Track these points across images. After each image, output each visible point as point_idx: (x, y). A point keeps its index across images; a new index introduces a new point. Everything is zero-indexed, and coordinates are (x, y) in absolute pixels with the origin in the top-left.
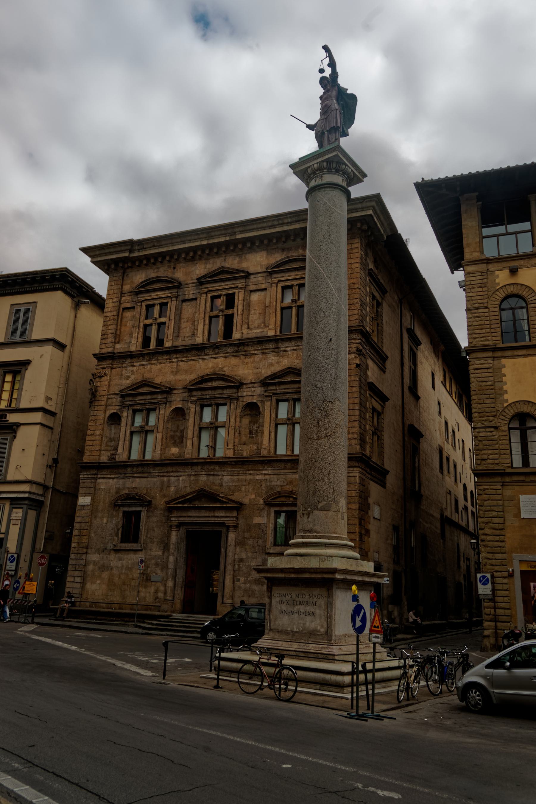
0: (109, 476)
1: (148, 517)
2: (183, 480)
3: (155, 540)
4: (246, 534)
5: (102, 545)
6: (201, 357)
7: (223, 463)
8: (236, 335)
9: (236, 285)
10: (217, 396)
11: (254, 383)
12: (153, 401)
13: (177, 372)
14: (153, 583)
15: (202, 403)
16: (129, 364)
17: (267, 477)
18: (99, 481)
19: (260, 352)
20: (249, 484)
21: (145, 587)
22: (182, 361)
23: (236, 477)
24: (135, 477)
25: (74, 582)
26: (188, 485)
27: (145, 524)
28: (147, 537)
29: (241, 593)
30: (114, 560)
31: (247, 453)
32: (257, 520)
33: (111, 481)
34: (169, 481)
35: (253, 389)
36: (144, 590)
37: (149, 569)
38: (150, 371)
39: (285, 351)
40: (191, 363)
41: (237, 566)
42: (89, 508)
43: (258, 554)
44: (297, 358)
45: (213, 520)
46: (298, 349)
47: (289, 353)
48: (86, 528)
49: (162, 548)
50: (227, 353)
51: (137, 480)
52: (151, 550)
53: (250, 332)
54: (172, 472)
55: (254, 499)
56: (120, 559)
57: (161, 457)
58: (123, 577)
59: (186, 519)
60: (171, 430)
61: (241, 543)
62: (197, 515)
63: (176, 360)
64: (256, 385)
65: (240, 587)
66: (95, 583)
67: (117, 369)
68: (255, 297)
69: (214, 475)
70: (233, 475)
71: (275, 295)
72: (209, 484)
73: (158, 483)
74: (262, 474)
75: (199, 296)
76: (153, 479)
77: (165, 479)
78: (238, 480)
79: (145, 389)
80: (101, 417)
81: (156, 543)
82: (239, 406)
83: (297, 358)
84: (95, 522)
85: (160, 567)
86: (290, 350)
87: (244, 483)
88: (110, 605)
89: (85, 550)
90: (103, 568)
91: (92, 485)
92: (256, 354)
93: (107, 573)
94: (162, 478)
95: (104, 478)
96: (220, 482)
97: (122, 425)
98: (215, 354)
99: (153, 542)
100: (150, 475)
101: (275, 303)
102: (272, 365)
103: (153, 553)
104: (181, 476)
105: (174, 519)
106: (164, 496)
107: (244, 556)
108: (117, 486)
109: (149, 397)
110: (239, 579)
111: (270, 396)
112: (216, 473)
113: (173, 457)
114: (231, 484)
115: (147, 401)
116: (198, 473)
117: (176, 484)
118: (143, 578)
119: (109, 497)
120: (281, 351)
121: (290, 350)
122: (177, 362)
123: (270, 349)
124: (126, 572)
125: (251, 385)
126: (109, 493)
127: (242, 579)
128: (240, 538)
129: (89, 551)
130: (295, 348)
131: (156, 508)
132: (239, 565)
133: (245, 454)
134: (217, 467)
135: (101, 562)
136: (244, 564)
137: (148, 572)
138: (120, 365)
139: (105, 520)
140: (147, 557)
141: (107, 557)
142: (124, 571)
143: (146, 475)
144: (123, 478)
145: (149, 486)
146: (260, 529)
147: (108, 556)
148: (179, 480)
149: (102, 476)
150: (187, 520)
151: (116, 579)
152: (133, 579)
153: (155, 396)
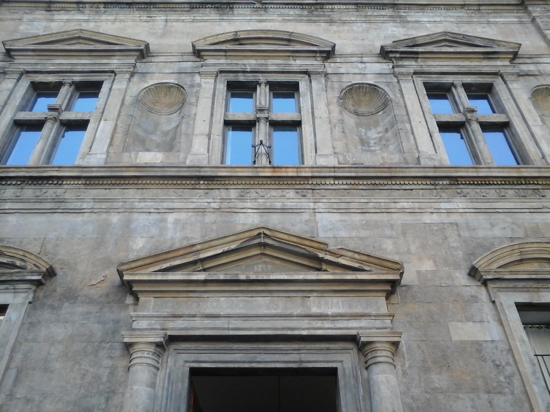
2: (177, 222)
11: (362, 56)
12: (96, 68)
13: (163, 35)
20: (404, 234)
23: (357, 218)
27: (13, 350)
32: (463, 332)
34: (127, 224)
40: (201, 24)
45: (304, 328)
55: (433, 272)
57: (106, 162)
60: (139, 126)
69: (284, 210)
70: (347, 211)
73: (90, 228)
74: (438, 211)
77: (115, 218)
78: (367, 225)
82: (333, 88)
86: (429, 22)
87: (388, 232)
92: (353, 22)
94: (104, 216)
100: (60, 207)
104: (171, 210)
114: (343, 234)
115: (79, 68)
120: (408, 22)
121: (429, 22)
122: (166, 21)
128: (416, 391)
131: (71, 296)
143: (48, 206)
145: (52, 235)
146: (484, 360)
148: (164, 220)
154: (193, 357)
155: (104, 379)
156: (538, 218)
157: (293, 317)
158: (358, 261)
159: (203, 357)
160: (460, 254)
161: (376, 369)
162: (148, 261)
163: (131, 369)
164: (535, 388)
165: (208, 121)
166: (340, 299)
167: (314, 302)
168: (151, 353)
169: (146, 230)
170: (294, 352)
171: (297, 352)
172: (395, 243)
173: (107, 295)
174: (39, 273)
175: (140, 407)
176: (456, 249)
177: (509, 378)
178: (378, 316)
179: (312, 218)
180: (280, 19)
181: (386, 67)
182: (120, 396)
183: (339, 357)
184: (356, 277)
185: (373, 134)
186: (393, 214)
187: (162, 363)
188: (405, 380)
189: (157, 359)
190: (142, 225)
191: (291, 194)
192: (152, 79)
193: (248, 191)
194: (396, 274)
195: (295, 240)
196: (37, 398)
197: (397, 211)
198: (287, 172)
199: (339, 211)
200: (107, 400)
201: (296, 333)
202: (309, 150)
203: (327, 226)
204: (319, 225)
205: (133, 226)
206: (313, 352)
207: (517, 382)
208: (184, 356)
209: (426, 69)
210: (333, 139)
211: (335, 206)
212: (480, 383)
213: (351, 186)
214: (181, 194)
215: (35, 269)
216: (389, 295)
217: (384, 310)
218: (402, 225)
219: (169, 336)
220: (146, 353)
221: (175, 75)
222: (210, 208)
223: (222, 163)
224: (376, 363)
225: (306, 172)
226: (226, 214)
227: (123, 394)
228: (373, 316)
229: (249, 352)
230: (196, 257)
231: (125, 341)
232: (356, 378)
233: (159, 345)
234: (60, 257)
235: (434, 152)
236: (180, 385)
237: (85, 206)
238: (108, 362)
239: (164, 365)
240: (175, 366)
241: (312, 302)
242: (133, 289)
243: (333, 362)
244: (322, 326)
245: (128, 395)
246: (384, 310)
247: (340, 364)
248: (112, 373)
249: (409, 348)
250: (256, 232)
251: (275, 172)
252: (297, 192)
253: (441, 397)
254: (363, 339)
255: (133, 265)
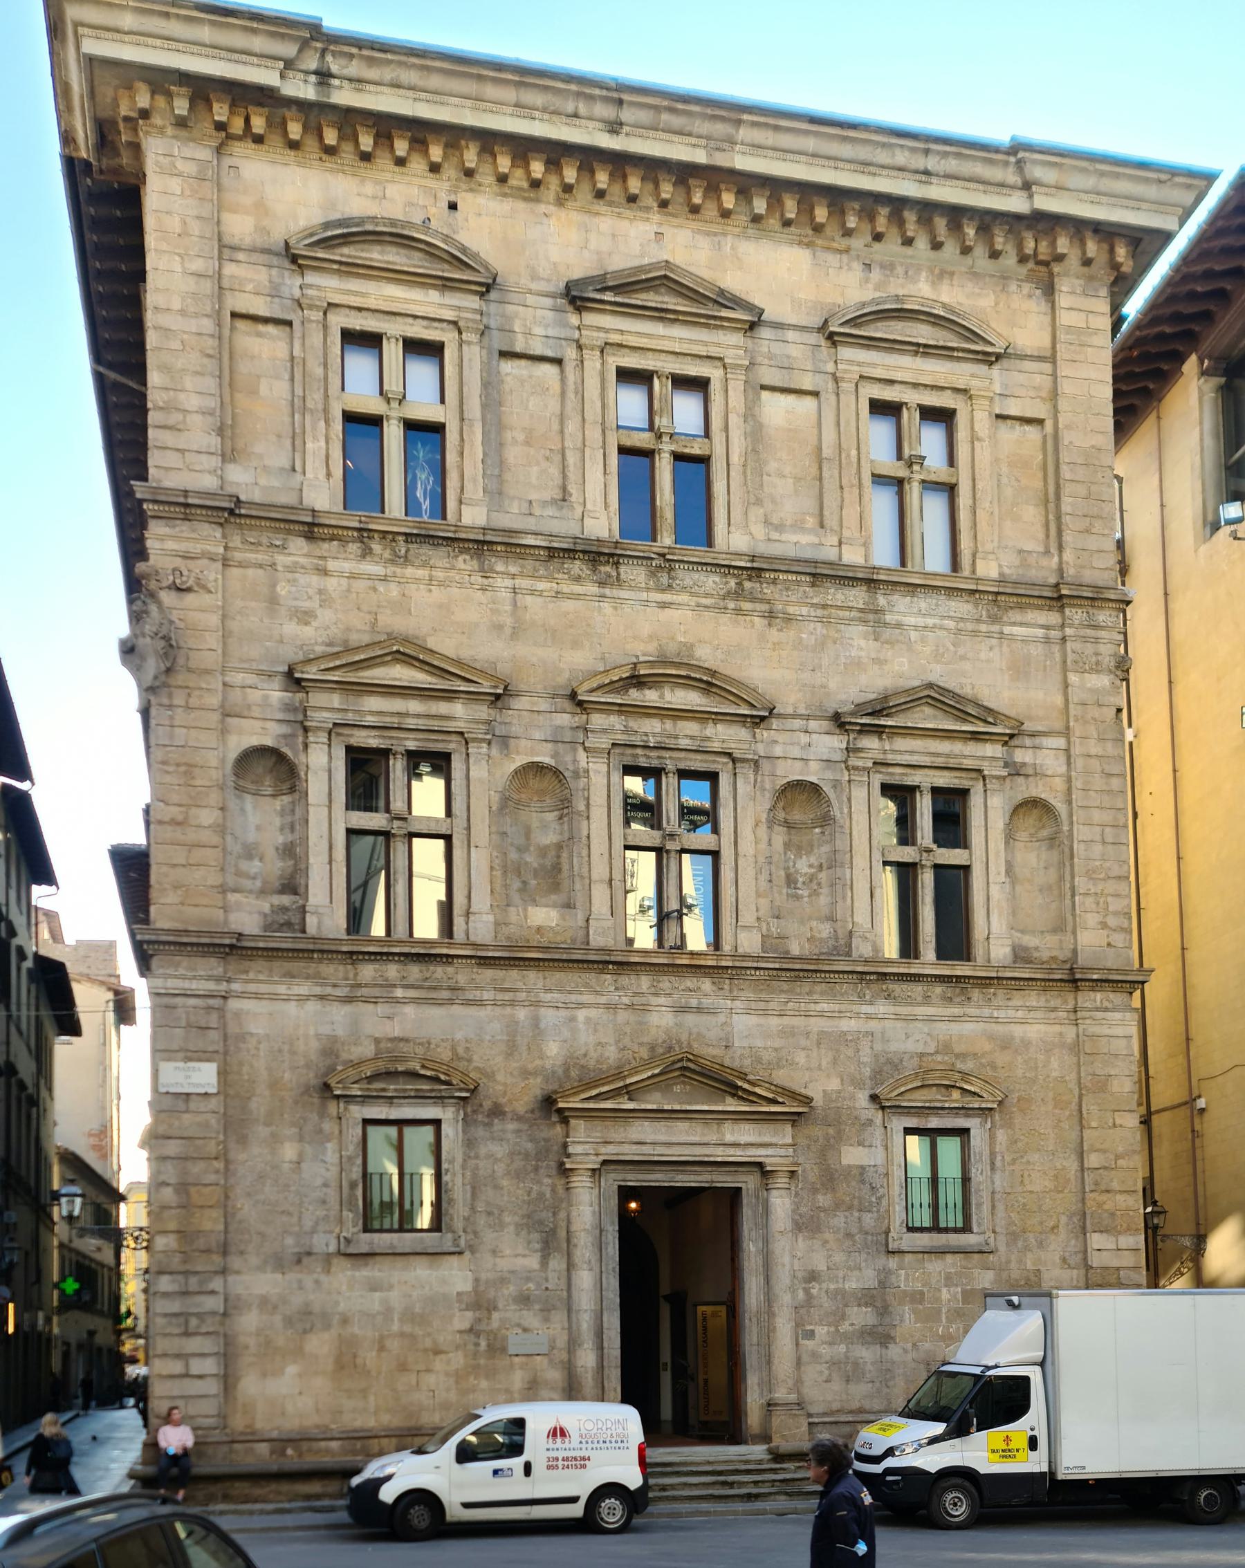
0: (282, 989)
1: (470, 1143)
2: (588, 1020)
3: (507, 1219)
4: (820, 1197)
5: (289, 1241)
6: (607, 591)
7: (717, 968)
8: (735, 536)
9: (714, 351)
10: (684, 743)
13: (516, 633)
14: (516, 1359)
15: (629, 761)
16: (302, 560)
17: (873, 1025)
18: (233, 1004)
19: (819, 612)
20: (819, 1044)
21: (491, 1374)
22: (533, 592)
23: (774, 1021)
24: (397, 1001)
25: (187, 1375)
26: (612, 1041)
27: (464, 1167)
28: (473, 1208)
29: (821, 1372)
30: (347, 1289)
31: (802, 948)
32: (852, 1156)
33: (292, 1008)
34: (536, 1022)
35: (805, 739)
36: (484, 1384)
37: (496, 1316)
38: (402, 606)
39: (899, 625)
40: (569, 605)
41: (801, 1295)
42: (213, 1104)
43: (864, 1256)
44: (937, 656)
45: (720, 1154)
46: (942, 628)
47: (914, 635)
48: (212, 1178)
49: (538, 1246)
50: (707, 595)
51: (409, 1010)
52: (494, 1252)
53: (775, 535)
54: (550, 991)
55: (839, 1092)
56: (374, 1287)
58: (394, 1345)
60: (512, 844)
61: (806, 1225)
62: (662, 1138)
63: (509, 582)
64: (813, 725)
65: (815, 1355)
66: (279, 1372)
67: (250, 572)
68: (776, 408)
69: (699, 1010)
70: (765, 1013)
71: (853, 424)
72: (684, 1038)
73: (496, 1026)
75: (570, 353)
76: (472, 1011)
77: (522, 1014)
79: (400, 674)
80: (212, 759)
81: (512, 1228)
82: (763, 789)
83: (937, 656)
84: (242, 1157)
85: (537, 1307)
88: (359, 1444)
89: (217, 1259)
90: (306, 1320)
91: (213, 1020)
93: (326, 1336)
94: (508, 1010)
95: (257, 996)
96: (722, 1035)
97: (312, 799)
98: (663, 591)
99: (502, 1226)
100: (456, 996)
101: (854, 453)
102: (858, 664)
103: (504, 1264)
104: (581, 1005)
106: (526, 1073)
107: (819, 1262)
108: (326, 1030)
109: (414, 706)
110: (813, 1332)
111: (864, 769)
112: (706, 1002)
113: (536, 940)
114: (759, 1043)
115: (411, 723)
117: (566, 1033)
118: (477, 1345)
119: (293, 1068)
122: (514, 590)
123: (850, 608)
124: (407, 1328)
125: (797, 723)
126: (293, 1053)
127: (821, 1331)
128: (803, 1209)
129: (235, 1262)
130: (930, 621)
131: (497, 1112)
132: (806, 1291)
133: (795, 950)
134: (707, 985)
135: (297, 1300)
136: (824, 1286)
137: (495, 1324)
138: (260, 557)
139: (289, 1151)
140: (483, 1276)
141: (317, 1282)
142: (396, 1327)
144: (348, 1000)
145: (459, 1036)
147: (324, 1278)
148: (573, 1019)
149: (252, 987)
150: (630, 1152)
151: (369, 1356)
152: (437, 1352)
153: (442, 708)
154: (620, 1176)
155: (548, 1195)
156: (955, 1028)
160: (867, 1072)
161: (774, 1193)
164: (897, 1208)
165: (607, 855)
172: (808, 1056)
173: (532, 1111)
174: (467, 1090)
176: (865, 1064)
177: (879, 1198)
180: (693, 601)
181: (837, 742)
183: (743, 1178)
185: (803, 866)
192: (518, 753)
196: (496, 1212)
200: (554, 1214)
201: (712, 1159)
202: (728, 914)
204: (735, 1030)
205: (542, 1026)
207: (884, 1202)
209: (890, 758)
210: (758, 895)
212: (856, 1202)
215: (462, 1085)
221: (550, 745)
234: (475, 1064)
237: (486, 996)
238: (547, 1181)
248: (553, 1191)
253: (822, 1214)
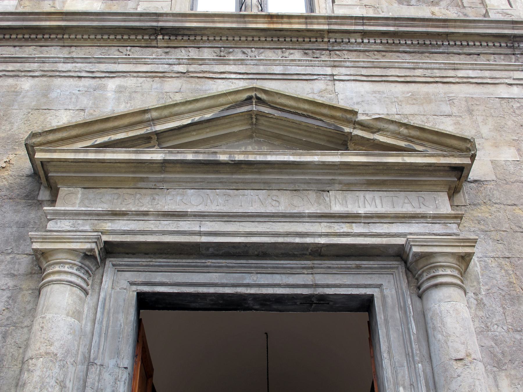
2: (120, 90)
20: (470, 112)
34: (45, 93)
45: (320, 233)
59: (151, 225)
70: (384, 80)
87: (446, 109)
104: (112, 74)
105: (76, 220)
116: (204, 68)
128: (499, 331)
157: (304, 217)
158: (406, 138)
159: (158, 277)
162: (74, 132)
163: (43, 291)
166: (377, 194)
167: (336, 197)
168: (75, 268)
169: (73, 100)
170: (305, 271)
171: (310, 271)
175: (56, 344)
178: (437, 218)
179: (330, 88)
182: (26, 330)
183: (375, 280)
184: (403, 160)
186: (452, 85)
187: (92, 285)
188: (480, 313)
189: (85, 277)
190: (68, 93)
191: (297, 55)
193: (231, 50)
194: (465, 157)
195: (306, 106)
197: (457, 80)
198: (290, 23)
199: (370, 79)
203: (352, 98)
206: (334, 271)
208: (128, 274)
211: (364, 72)
213: (387, 46)
214: (128, 53)
216: (453, 192)
217: (446, 208)
218: (467, 100)
219: (106, 242)
220: (66, 266)
222: (172, 72)
223: (192, 9)
224: (436, 286)
225: (318, 24)
226: (196, 80)
227: (30, 328)
228: (430, 217)
229: (231, 270)
230: (149, 128)
231: (34, 247)
232: (404, 309)
233: (88, 255)
235: (509, 7)
236: (121, 317)
239: (97, 288)
240: (112, 288)
241: (333, 198)
242: (49, 175)
243: (366, 286)
244: (350, 231)
245: (36, 327)
246: (446, 208)
247: (377, 290)
249: (486, 267)
250: (245, 96)
251: (273, 23)
252: (306, 53)
254: (415, 249)
255: (51, 137)
